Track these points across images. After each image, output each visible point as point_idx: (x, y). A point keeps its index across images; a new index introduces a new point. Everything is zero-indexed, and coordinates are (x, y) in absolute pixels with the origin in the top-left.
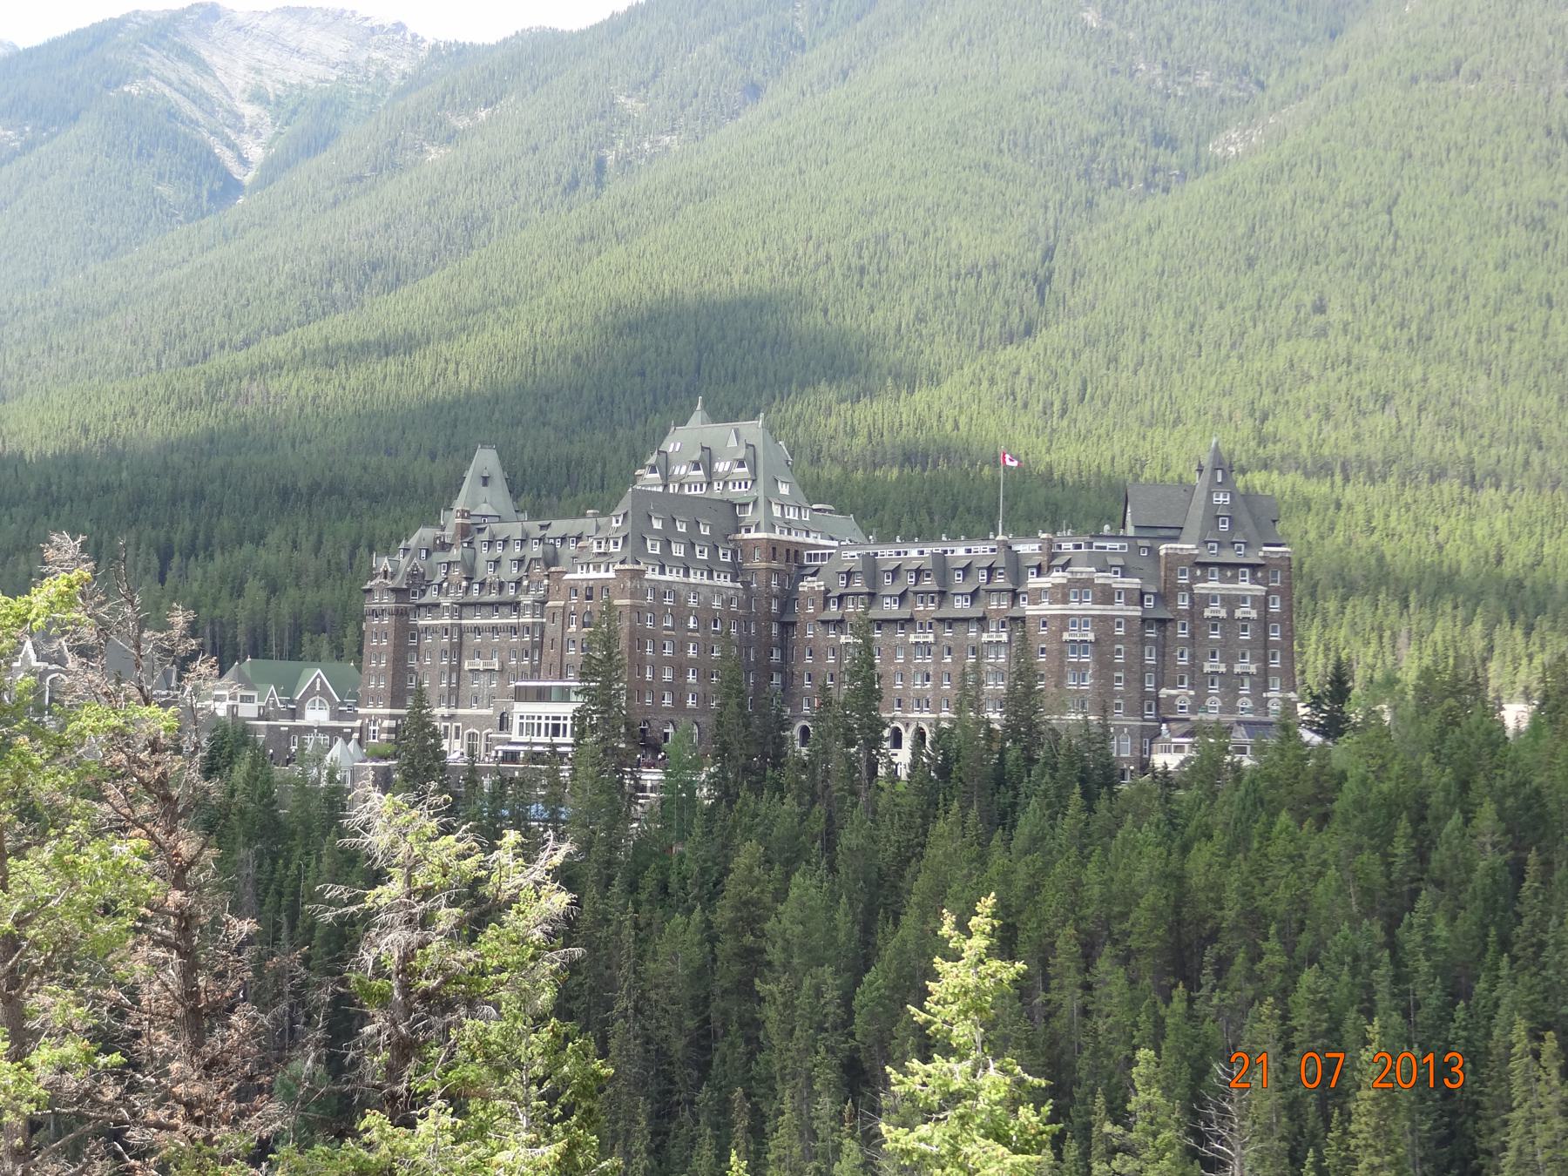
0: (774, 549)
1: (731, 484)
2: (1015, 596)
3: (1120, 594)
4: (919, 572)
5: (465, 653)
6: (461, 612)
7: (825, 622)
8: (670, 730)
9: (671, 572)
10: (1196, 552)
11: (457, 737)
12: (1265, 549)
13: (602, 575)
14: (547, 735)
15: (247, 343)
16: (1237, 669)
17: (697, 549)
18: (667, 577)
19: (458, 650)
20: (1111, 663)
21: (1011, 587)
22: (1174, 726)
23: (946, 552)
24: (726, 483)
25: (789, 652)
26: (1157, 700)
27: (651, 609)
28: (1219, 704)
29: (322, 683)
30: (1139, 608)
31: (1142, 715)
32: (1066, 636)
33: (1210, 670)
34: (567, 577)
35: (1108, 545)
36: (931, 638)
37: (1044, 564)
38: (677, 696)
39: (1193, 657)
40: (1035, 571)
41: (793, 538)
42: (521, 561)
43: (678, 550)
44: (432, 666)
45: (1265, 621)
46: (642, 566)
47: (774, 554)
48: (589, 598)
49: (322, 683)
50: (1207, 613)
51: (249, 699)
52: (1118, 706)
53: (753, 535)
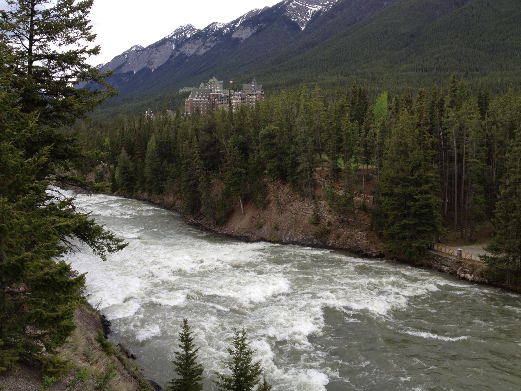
43: (200, 96)
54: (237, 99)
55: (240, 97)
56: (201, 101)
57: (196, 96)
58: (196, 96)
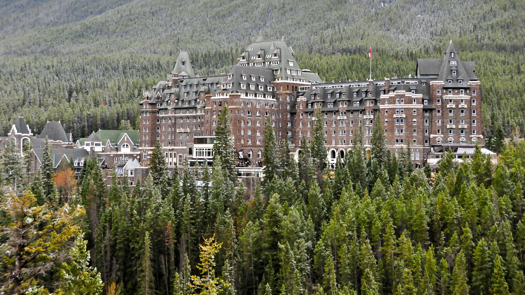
0: (288, 86)
1: (256, 64)
2: (376, 101)
3: (414, 100)
4: (340, 93)
5: (177, 126)
6: (175, 111)
7: (306, 113)
8: (251, 153)
9: (250, 95)
10: (444, 83)
11: (175, 157)
12: (470, 82)
13: (225, 97)
14: (206, 156)
15: (100, 12)
16: (460, 127)
17: (260, 87)
18: (248, 97)
19: (174, 125)
20: (412, 125)
21: (374, 98)
22: (436, 148)
23: (350, 86)
24: (270, 63)
25: (294, 124)
26: (430, 139)
27: (243, 109)
28: (453, 140)
29: (127, 138)
30: (422, 105)
31: (424, 144)
32: (395, 116)
33: (449, 127)
34: (212, 98)
35: (410, 82)
36: (345, 118)
37: (387, 90)
38: (253, 140)
39: (443, 122)
40: (383, 92)
41: (295, 82)
42: (196, 92)
43: (253, 88)
44: (165, 131)
45: (470, 110)
46: (239, 94)
47: (288, 88)
48: (220, 105)
49: (127, 138)
50: (448, 106)
51: (99, 145)
52: (415, 141)
53: (280, 81)
54: (410, 101)
55: (414, 96)
56: (259, 101)
57: (244, 87)
58: (244, 87)
